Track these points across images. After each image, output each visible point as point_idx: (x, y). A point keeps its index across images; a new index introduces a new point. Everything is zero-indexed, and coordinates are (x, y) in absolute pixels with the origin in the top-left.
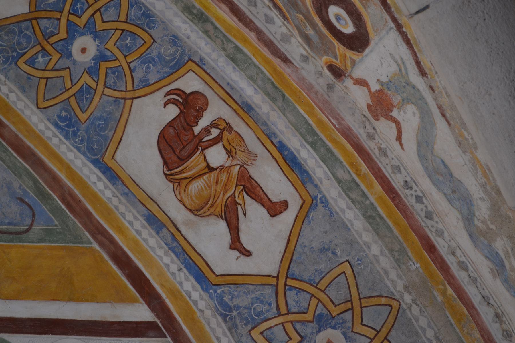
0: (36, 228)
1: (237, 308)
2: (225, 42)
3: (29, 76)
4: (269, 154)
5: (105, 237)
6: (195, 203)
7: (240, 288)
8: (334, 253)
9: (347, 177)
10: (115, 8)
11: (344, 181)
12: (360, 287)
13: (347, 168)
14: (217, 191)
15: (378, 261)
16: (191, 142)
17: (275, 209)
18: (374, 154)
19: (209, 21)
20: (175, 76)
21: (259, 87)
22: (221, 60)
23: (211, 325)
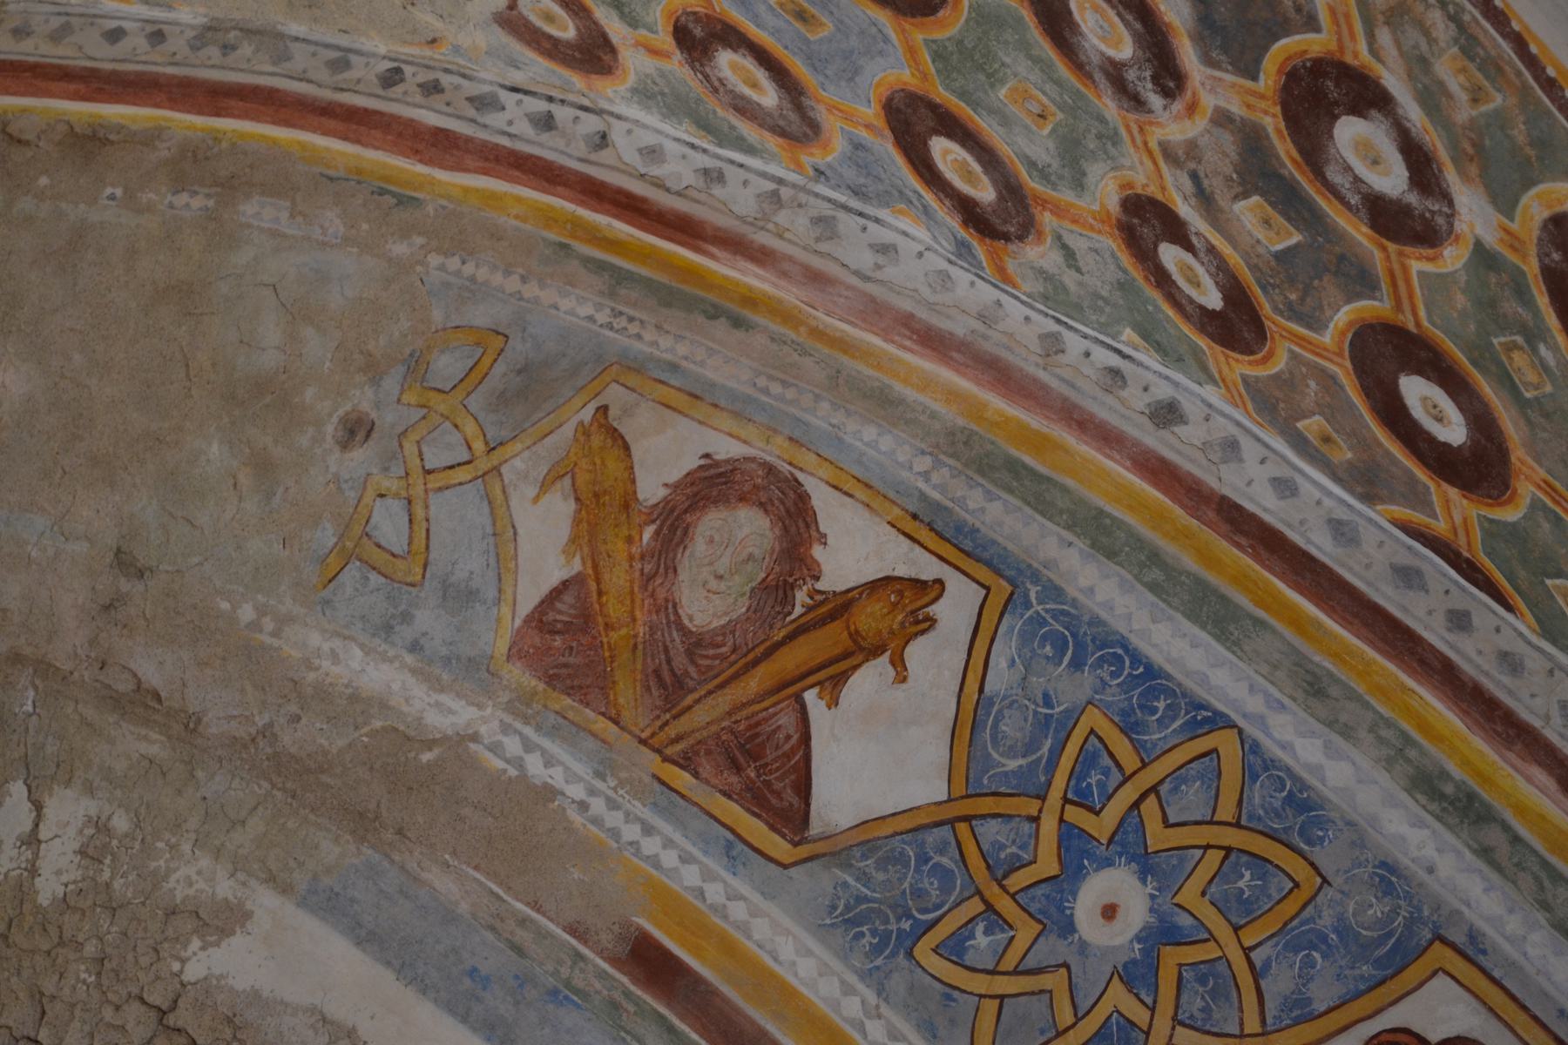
2: (1547, 883)
3: (948, 990)
19: (1495, 820)
20: (1394, 988)
22: (1536, 937)
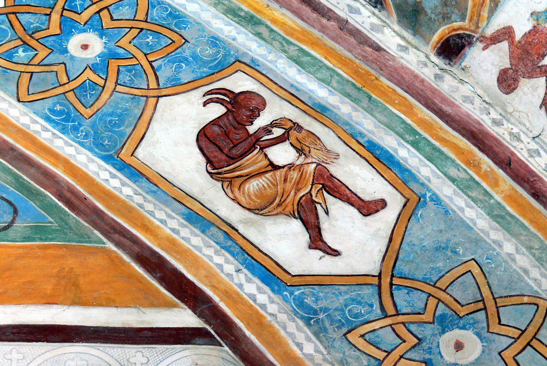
0: (19, 224)
1: (325, 310)
2: (285, 44)
3: (4, 69)
4: (355, 153)
5: (124, 236)
6: (255, 202)
7: (328, 289)
8: (455, 253)
9: (462, 175)
10: (130, 7)
11: (459, 180)
12: (493, 287)
13: (461, 167)
14: (286, 190)
15: (514, 260)
16: (245, 140)
17: (369, 208)
18: (504, 139)
19: (263, 24)
20: (218, 76)
21: (334, 89)
22: (281, 61)
23: (288, 330)
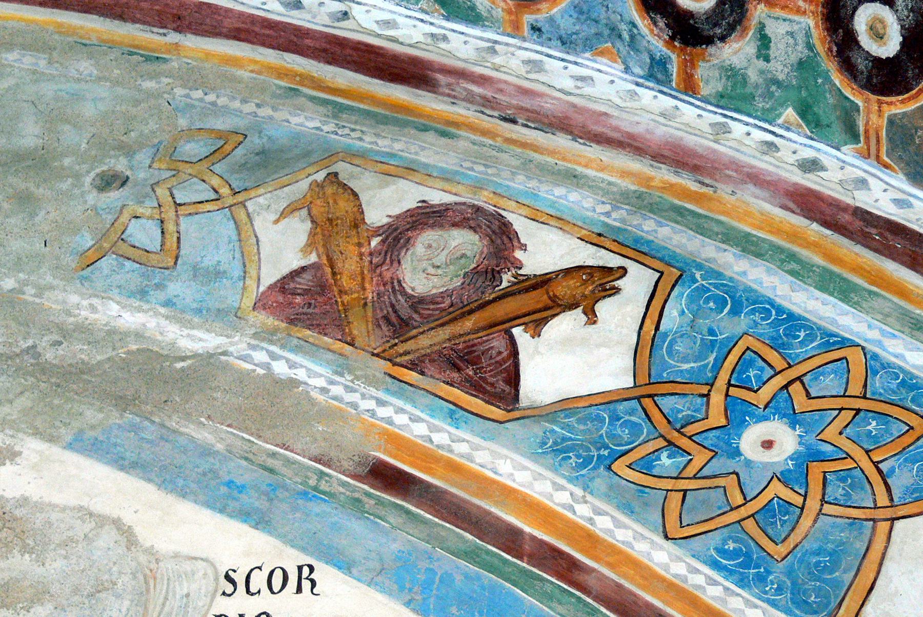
10: (836, 375)
